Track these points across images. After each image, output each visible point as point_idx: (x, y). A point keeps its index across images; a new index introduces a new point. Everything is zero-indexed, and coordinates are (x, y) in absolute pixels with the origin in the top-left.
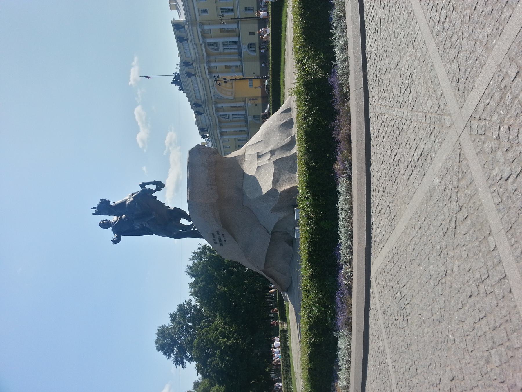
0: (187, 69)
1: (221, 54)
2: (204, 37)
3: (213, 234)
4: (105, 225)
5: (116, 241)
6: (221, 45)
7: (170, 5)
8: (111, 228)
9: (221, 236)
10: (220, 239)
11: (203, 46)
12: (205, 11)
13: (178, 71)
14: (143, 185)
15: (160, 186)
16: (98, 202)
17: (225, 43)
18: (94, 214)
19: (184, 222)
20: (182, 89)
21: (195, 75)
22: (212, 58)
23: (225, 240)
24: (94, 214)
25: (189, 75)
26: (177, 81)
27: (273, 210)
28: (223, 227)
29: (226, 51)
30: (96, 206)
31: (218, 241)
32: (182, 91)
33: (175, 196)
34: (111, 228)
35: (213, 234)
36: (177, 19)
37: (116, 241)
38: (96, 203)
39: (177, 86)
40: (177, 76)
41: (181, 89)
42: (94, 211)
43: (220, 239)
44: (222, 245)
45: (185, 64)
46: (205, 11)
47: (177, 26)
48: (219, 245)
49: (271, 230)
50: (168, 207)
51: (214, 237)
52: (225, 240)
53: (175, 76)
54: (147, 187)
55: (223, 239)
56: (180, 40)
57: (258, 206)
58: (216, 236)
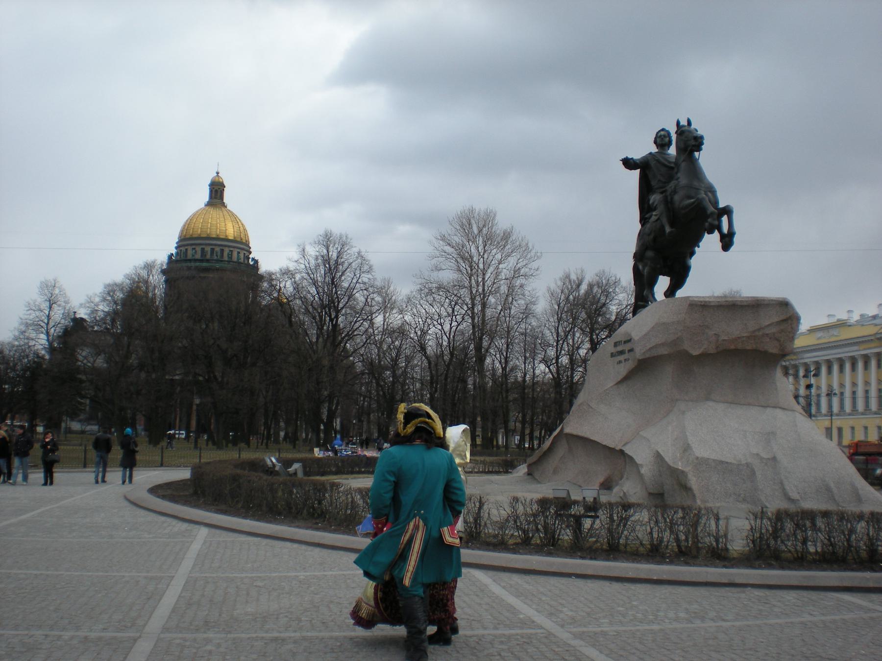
3: (629, 341)
4: (662, 140)
5: (628, 163)
8: (654, 149)
9: (626, 356)
10: (621, 353)
14: (727, 211)
15: (727, 242)
18: (678, 123)
19: (663, 283)
23: (620, 362)
24: (678, 123)
27: (658, 456)
28: (639, 361)
30: (693, 127)
31: (619, 348)
33: (711, 270)
34: (654, 149)
35: (629, 341)
37: (628, 163)
38: (700, 127)
42: (684, 122)
43: (621, 353)
44: (612, 355)
48: (613, 350)
49: (628, 450)
50: (692, 253)
51: (625, 342)
52: (620, 362)
54: (725, 219)
55: (621, 358)
57: (670, 428)
58: (627, 347)
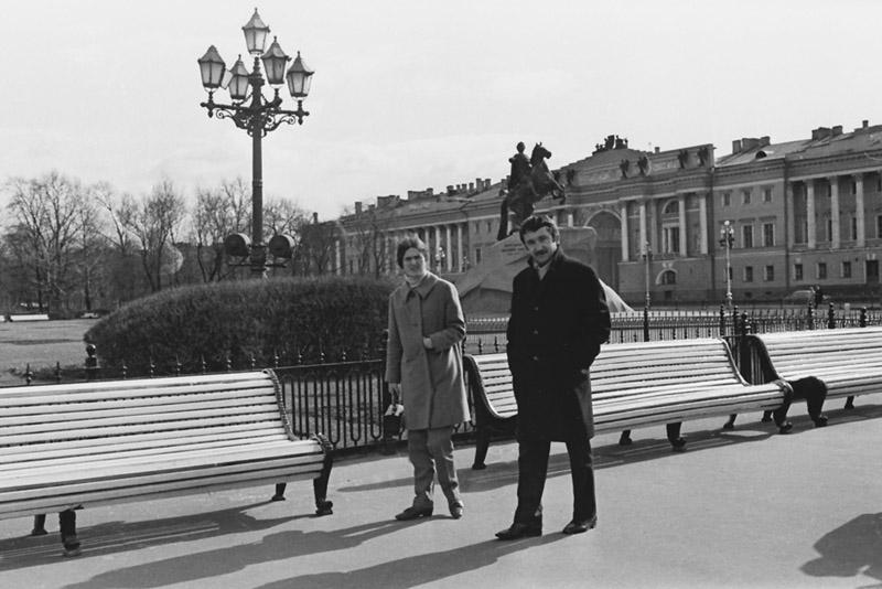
0: (634, 161)
1: (659, 224)
2: (688, 197)
6: (674, 225)
7: (739, 141)
8: (517, 152)
11: (672, 194)
12: (727, 203)
13: (629, 147)
16: (549, 149)
17: (676, 231)
20: (598, 151)
21: (624, 176)
22: (653, 209)
25: (625, 166)
26: (614, 145)
29: (663, 232)
32: (595, 150)
36: (717, 154)
39: (604, 143)
40: (621, 144)
41: (600, 150)
45: (643, 159)
46: (727, 203)
47: (705, 152)
53: (621, 141)
56: (683, 155)
